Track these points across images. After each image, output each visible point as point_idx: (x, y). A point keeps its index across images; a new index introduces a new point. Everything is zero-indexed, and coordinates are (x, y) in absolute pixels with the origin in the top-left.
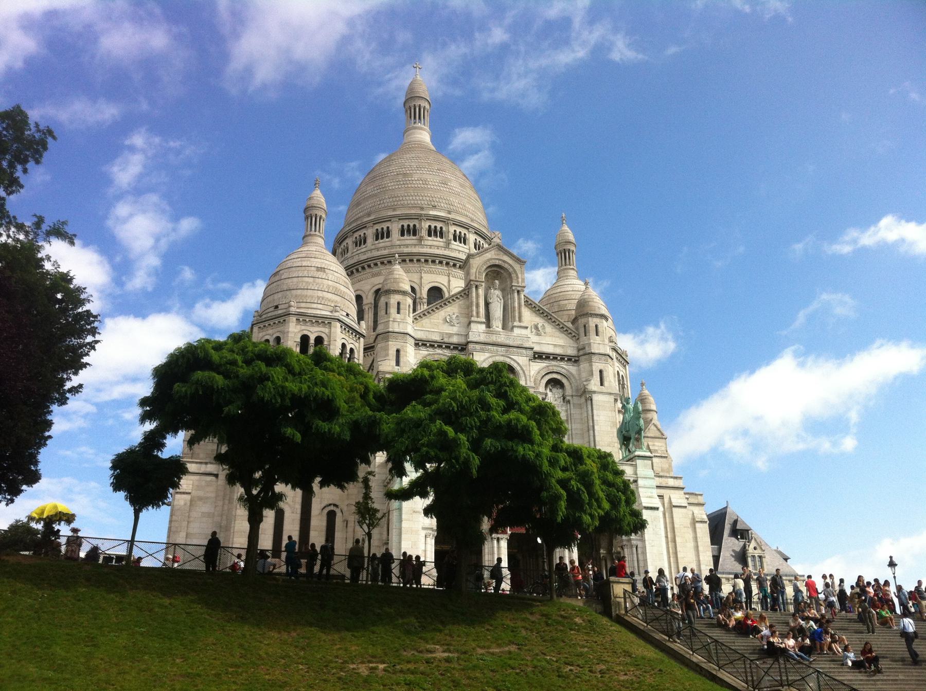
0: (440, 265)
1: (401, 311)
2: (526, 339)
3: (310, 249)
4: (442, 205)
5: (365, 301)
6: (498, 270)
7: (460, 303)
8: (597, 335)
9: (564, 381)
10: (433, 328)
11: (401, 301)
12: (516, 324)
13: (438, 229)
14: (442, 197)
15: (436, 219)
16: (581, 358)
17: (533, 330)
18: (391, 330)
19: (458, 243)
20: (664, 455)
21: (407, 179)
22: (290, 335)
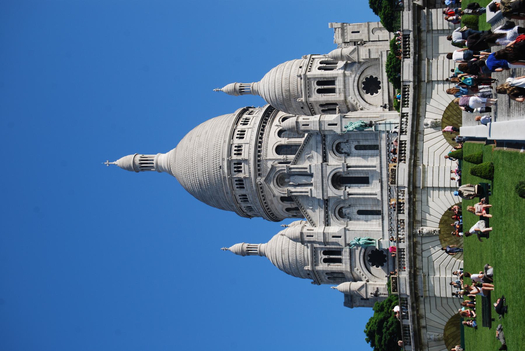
0: (260, 165)
1: (311, 235)
3: (270, 255)
4: (218, 162)
5: (291, 207)
7: (301, 200)
8: (308, 125)
9: (336, 143)
10: (317, 215)
11: (306, 235)
12: (308, 170)
13: (236, 166)
14: (213, 162)
15: (229, 168)
16: (322, 134)
18: (322, 241)
19: (243, 152)
20: (368, 51)
21: (204, 184)
22: (325, 269)
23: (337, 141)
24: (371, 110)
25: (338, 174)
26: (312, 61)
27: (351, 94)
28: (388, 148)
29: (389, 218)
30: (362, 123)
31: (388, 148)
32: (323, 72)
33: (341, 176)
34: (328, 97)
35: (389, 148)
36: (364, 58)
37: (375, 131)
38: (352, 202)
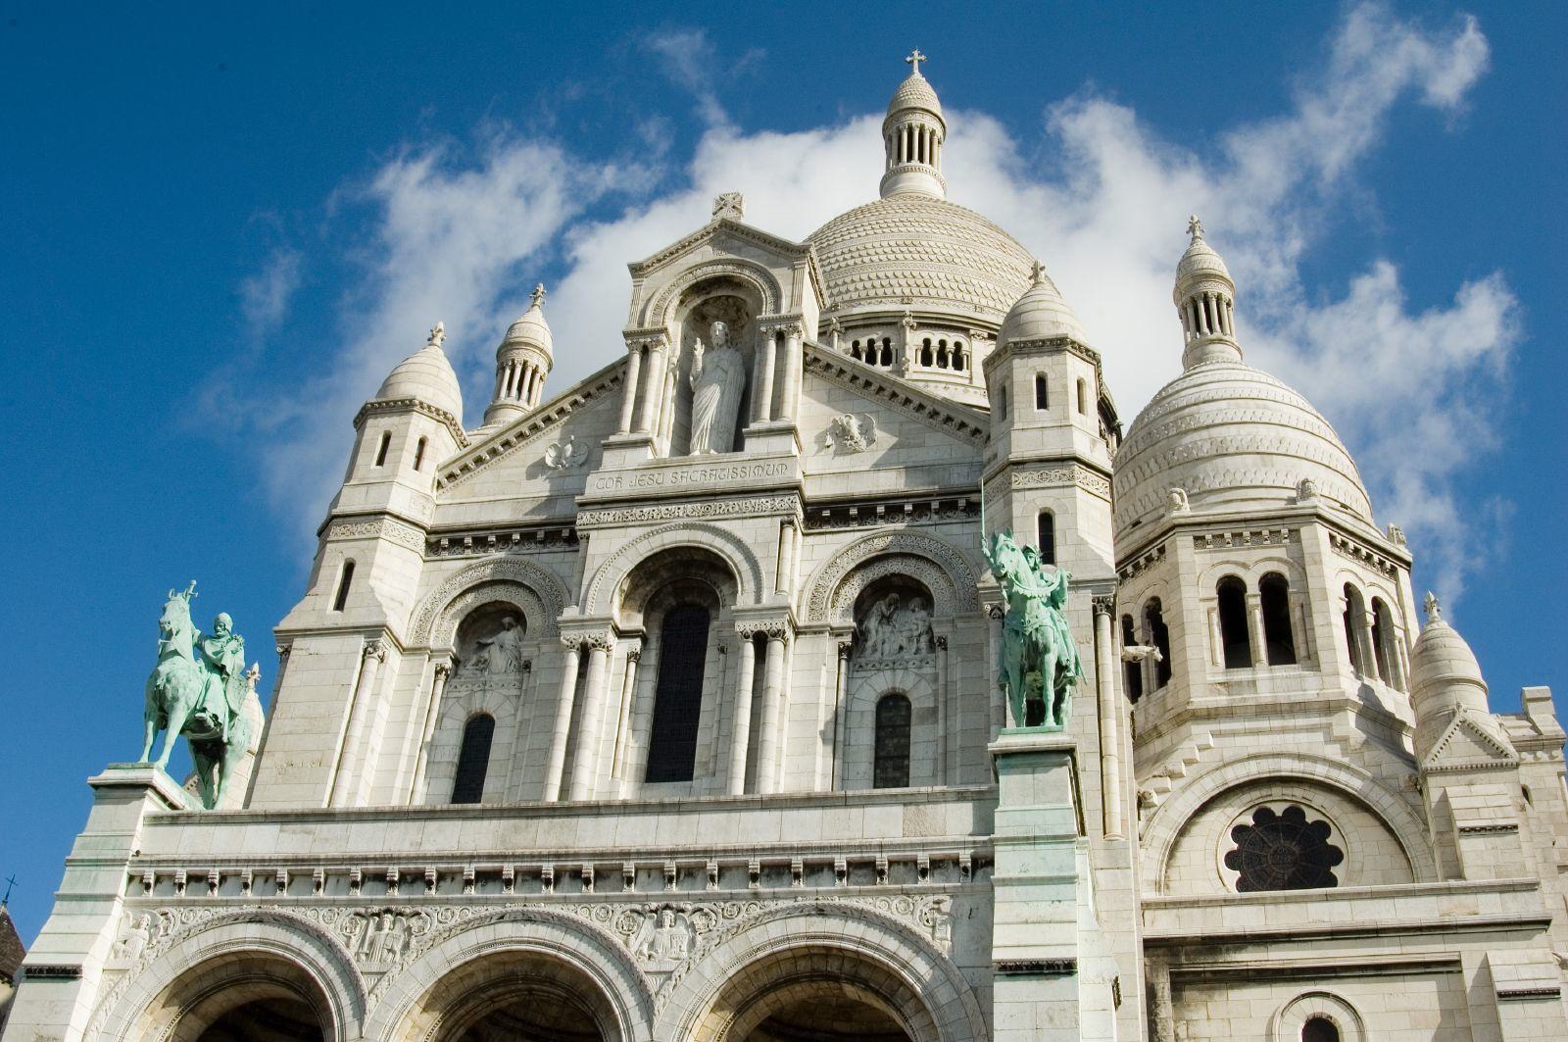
1: (388, 456)
2: (777, 462)
6: (731, 293)
7: (600, 407)
8: (1042, 403)
9: (929, 578)
10: (503, 494)
12: (765, 421)
13: (879, 345)
14: (898, 274)
15: (871, 322)
17: (829, 441)
23: (943, 584)
24: (1142, 852)
25: (724, 590)
26: (1381, 563)
27: (1228, 741)
28: (841, 861)
29: (286, 861)
30: (1061, 668)
31: (841, 861)
32: (1337, 606)
33: (713, 613)
34: (1205, 630)
35: (841, 875)
36: (1454, 803)
37: (996, 756)
38: (540, 678)
